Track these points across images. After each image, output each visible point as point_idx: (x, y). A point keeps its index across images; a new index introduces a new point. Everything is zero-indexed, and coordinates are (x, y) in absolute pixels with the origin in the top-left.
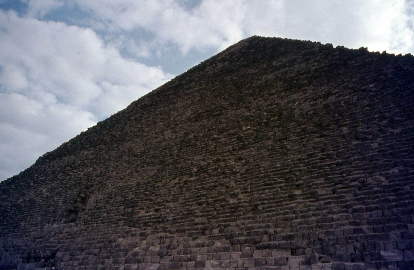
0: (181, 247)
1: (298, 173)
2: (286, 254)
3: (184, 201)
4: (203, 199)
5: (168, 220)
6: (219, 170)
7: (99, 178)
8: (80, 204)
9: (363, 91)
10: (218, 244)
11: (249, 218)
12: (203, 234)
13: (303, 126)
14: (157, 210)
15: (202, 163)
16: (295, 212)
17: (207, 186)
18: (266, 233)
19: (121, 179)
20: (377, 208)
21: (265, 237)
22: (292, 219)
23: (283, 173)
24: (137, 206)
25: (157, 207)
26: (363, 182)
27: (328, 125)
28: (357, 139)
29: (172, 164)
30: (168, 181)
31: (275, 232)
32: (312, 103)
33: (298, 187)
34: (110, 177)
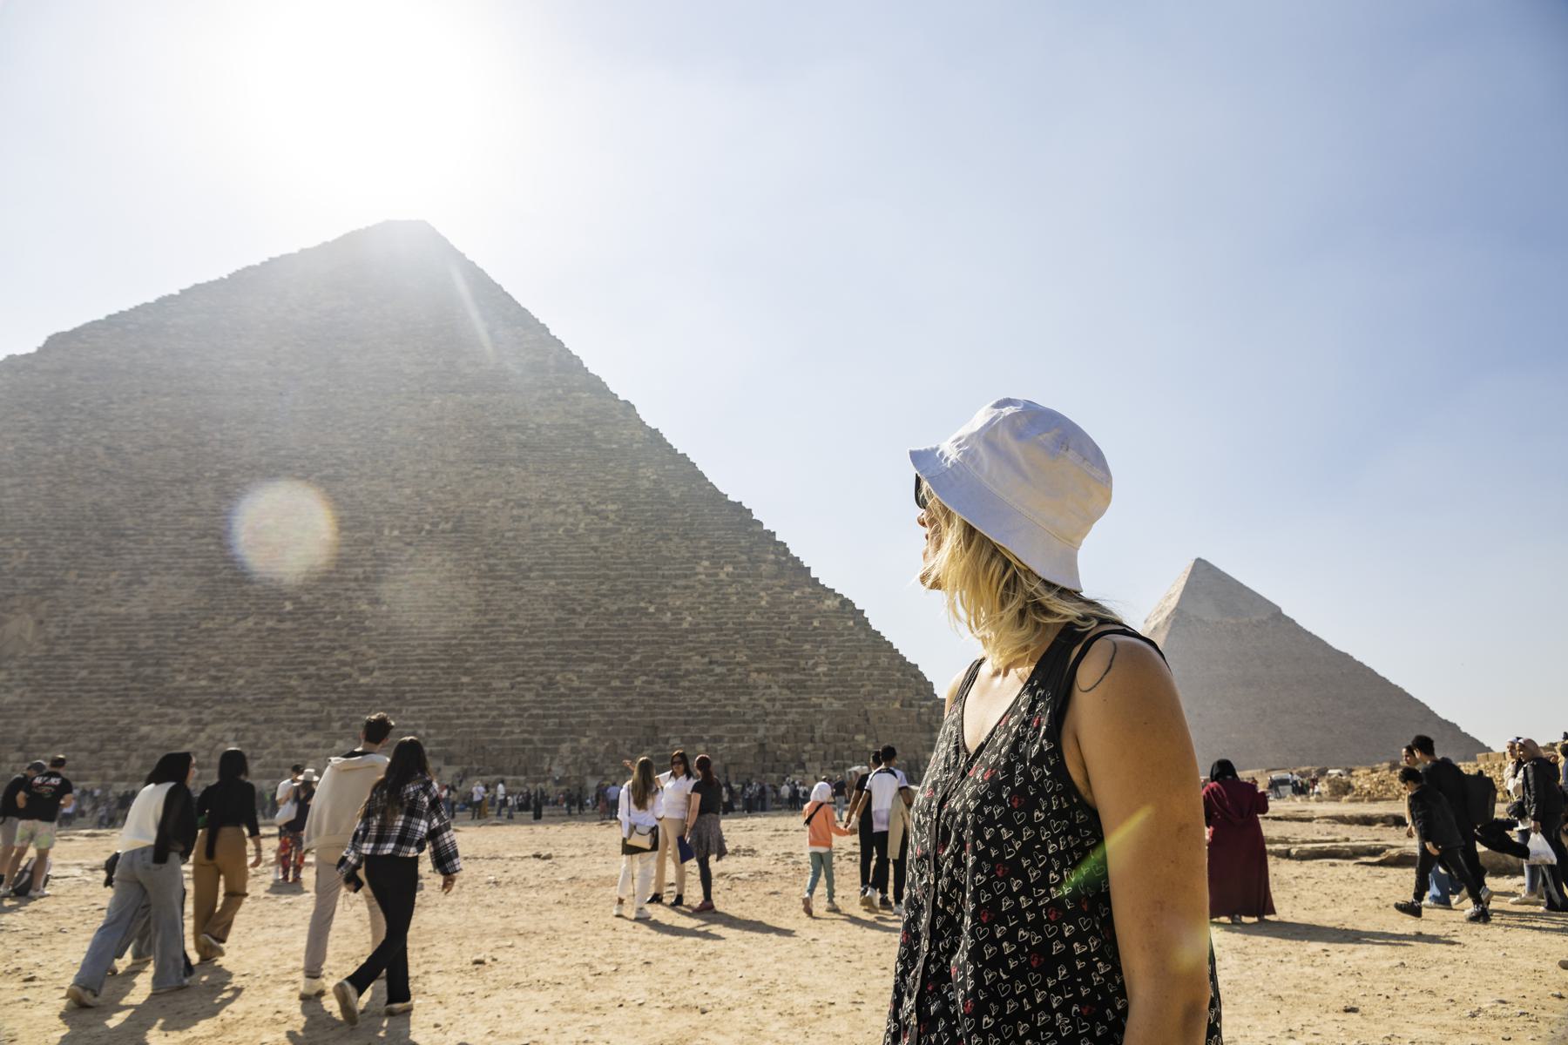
0: (277, 747)
1: (470, 649)
3: (271, 668)
4: (311, 669)
5: (244, 700)
6: (338, 618)
7: (29, 580)
9: (597, 513)
13: (492, 561)
14: (216, 679)
15: (306, 598)
16: (457, 710)
17: (317, 645)
19: (98, 592)
20: (555, 716)
22: (451, 718)
23: (449, 645)
24: (168, 665)
25: (213, 672)
26: (550, 678)
28: (563, 607)
29: (232, 581)
30: (232, 619)
31: (428, 735)
32: (515, 512)
33: (467, 672)
34: (64, 582)
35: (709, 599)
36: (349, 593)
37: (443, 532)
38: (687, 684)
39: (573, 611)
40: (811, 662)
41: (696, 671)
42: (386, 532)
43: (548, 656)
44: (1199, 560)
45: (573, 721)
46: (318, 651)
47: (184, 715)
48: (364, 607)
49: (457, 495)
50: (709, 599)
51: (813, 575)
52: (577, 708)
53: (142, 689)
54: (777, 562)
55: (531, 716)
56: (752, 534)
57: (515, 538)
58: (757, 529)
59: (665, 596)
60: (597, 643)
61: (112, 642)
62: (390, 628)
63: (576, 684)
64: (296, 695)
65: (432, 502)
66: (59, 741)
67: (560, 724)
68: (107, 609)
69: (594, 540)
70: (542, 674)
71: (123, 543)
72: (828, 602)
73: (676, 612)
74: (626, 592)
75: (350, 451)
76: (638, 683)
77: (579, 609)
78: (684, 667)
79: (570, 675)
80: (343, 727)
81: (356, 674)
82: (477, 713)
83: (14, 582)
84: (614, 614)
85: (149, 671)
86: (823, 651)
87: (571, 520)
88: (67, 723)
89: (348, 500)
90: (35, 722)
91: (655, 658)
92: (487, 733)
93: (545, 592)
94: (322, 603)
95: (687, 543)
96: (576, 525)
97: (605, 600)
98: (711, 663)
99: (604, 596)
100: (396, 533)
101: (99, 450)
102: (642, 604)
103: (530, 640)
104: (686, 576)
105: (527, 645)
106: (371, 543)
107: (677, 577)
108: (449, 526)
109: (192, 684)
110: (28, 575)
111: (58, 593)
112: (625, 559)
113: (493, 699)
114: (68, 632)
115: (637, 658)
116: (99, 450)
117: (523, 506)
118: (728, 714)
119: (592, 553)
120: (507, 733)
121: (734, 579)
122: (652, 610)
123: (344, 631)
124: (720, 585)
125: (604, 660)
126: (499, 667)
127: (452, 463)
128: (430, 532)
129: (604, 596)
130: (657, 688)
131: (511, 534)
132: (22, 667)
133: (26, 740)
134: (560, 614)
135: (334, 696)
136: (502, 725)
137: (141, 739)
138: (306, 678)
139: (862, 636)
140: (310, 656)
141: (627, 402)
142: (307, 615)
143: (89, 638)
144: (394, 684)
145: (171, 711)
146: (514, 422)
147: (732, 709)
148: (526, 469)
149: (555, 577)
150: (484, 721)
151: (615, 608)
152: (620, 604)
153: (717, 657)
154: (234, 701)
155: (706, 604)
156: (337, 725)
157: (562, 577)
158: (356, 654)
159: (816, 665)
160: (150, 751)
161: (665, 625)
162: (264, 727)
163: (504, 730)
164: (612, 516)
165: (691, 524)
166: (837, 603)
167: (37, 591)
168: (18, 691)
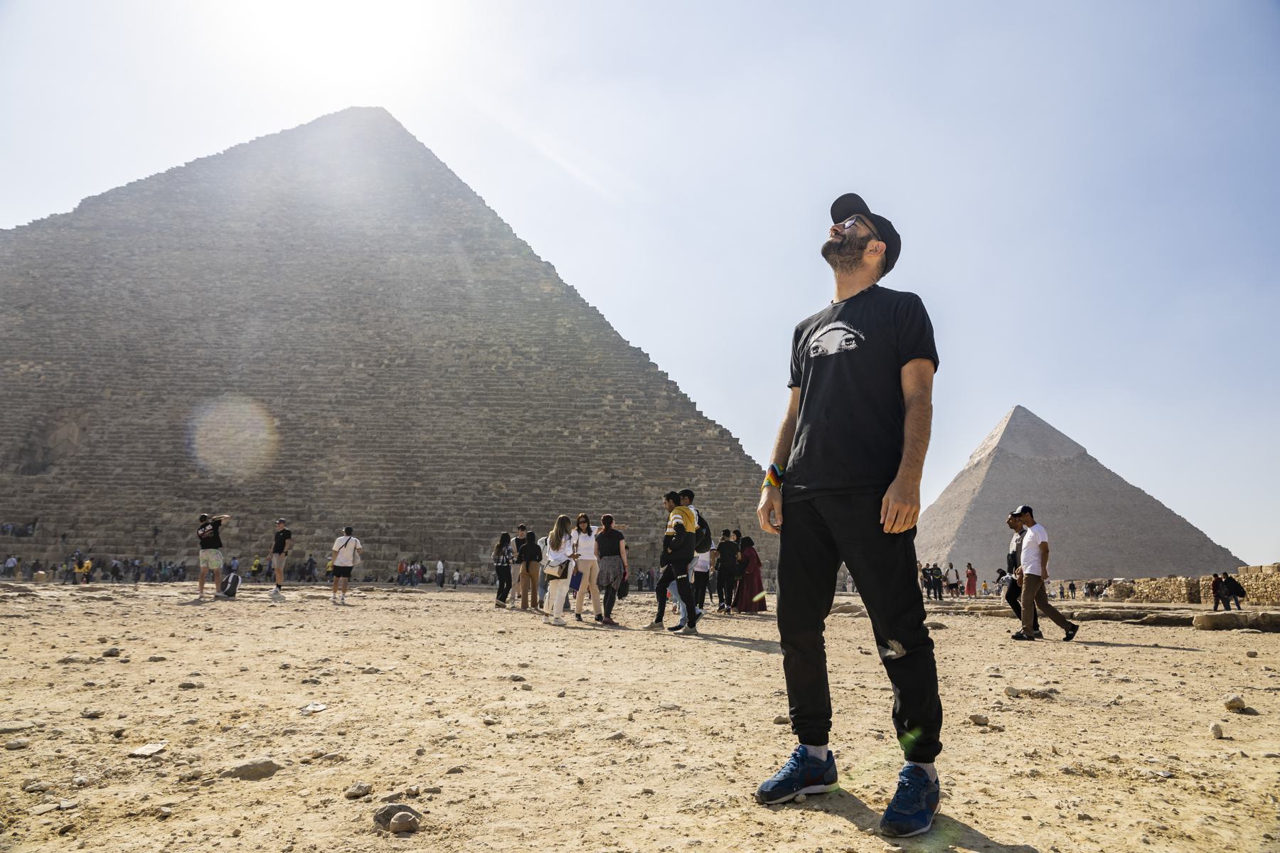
1: (421, 461)
2: (396, 550)
4: (295, 473)
7: (74, 396)
8: (37, 439)
10: (318, 532)
11: (358, 507)
12: (298, 519)
13: (438, 391)
15: (290, 416)
17: (300, 454)
18: (377, 526)
19: (128, 407)
20: (488, 516)
21: (376, 531)
22: (406, 515)
27: (468, 398)
28: (494, 429)
30: (232, 431)
33: (418, 479)
34: (102, 398)
35: (613, 426)
36: (325, 413)
37: (399, 366)
38: (593, 494)
39: (503, 433)
40: (694, 479)
41: (601, 484)
42: (353, 365)
43: (483, 468)
44: (1019, 407)
45: (502, 520)
46: (300, 458)
47: (196, 505)
48: (336, 425)
49: (410, 337)
50: (613, 426)
51: (698, 409)
52: (505, 510)
53: (164, 484)
54: (668, 398)
55: (469, 515)
56: (648, 374)
57: (456, 373)
58: (652, 370)
59: (577, 422)
60: (522, 459)
61: (140, 446)
62: (357, 442)
63: (505, 491)
64: (284, 493)
65: (390, 341)
66: (102, 522)
67: (492, 522)
68: (135, 420)
69: (520, 375)
70: (478, 482)
71: (146, 368)
72: (710, 431)
73: (586, 436)
74: (545, 419)
75: (324, 298)
76: (554, 491)
77: (508, 431)
78: (591, 480)
79: (500, 484)
80: (321, 519)
81: (330, 478)
82: (426, 511)
83: (62, 397)
84: (536, 436)
85: (169, 470)
86: (704, 470)
87: (501, 359)
88: (107, 508)
89: (322, 338)
90: (83, 507)
91: (568, 472)
92: (433, 527)
93: (481, 416)
94: (303, 420)
95: (595, 380)
96: (506, 364)
97: (528, 425)
98: (613, 477)
99: (528, 421)
100: (361, 366)
101: (125, 293)
102: (559, 429)
103: (468, 455)
104: (594, 407)
105: (466, 459)
106: (341, 373)
107: (587, 407)
108: (403, 361)
109: (202, 481)
110: (74, 392)
111: (97, 406)
112: (545, 392)
113: (439, 500)
114: (105, 438)
115: (554, 471)
116: (125, 293)
117: (463, 347)
118: (627, 519)
119: (518, 386)
120: (450, 528)
121: (633, 410)
122: (566, 433)
123: (321, 444)
124: (622, 415)
125: (528, 473)
126: (443, 475)
127: (406, 310)
128: (388, 366)
129: (528, 421)
130: (569, 496)
131: (453, 369)
132: (71, 464)
133: (76, 521)
134: (491, 435)
135: (314, 494)
136: (446, 521)
137: (164, 523)
138: (291, 479)
139: (737, 460)
140: (294, 463)
141: (548, 263)
142: (292, 429)
143: (122, 443)
144: (360, 486)
145: (187, 502)
146: (456, 278)
147: (629, 515)
148: (465, 317)
149: (488, 405)
150: (431, 518)
151: (537, 431)
152: (541, 428)
153: (618, 473)
154: (236, 496)
155: (610, 430)
156: (316, 517)
157: (493, 405)
158: (330, 462)
159: (698, 482)
160: (171, 533)
161: (576, 446)
162: (259, 517)
163: (447, 525)
164: (535, 357)
165: (599, 365)
166: (716, 432)
167: (81, 405)
168: (69, 483)
